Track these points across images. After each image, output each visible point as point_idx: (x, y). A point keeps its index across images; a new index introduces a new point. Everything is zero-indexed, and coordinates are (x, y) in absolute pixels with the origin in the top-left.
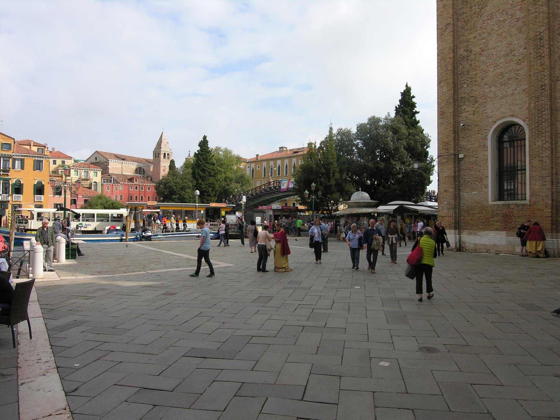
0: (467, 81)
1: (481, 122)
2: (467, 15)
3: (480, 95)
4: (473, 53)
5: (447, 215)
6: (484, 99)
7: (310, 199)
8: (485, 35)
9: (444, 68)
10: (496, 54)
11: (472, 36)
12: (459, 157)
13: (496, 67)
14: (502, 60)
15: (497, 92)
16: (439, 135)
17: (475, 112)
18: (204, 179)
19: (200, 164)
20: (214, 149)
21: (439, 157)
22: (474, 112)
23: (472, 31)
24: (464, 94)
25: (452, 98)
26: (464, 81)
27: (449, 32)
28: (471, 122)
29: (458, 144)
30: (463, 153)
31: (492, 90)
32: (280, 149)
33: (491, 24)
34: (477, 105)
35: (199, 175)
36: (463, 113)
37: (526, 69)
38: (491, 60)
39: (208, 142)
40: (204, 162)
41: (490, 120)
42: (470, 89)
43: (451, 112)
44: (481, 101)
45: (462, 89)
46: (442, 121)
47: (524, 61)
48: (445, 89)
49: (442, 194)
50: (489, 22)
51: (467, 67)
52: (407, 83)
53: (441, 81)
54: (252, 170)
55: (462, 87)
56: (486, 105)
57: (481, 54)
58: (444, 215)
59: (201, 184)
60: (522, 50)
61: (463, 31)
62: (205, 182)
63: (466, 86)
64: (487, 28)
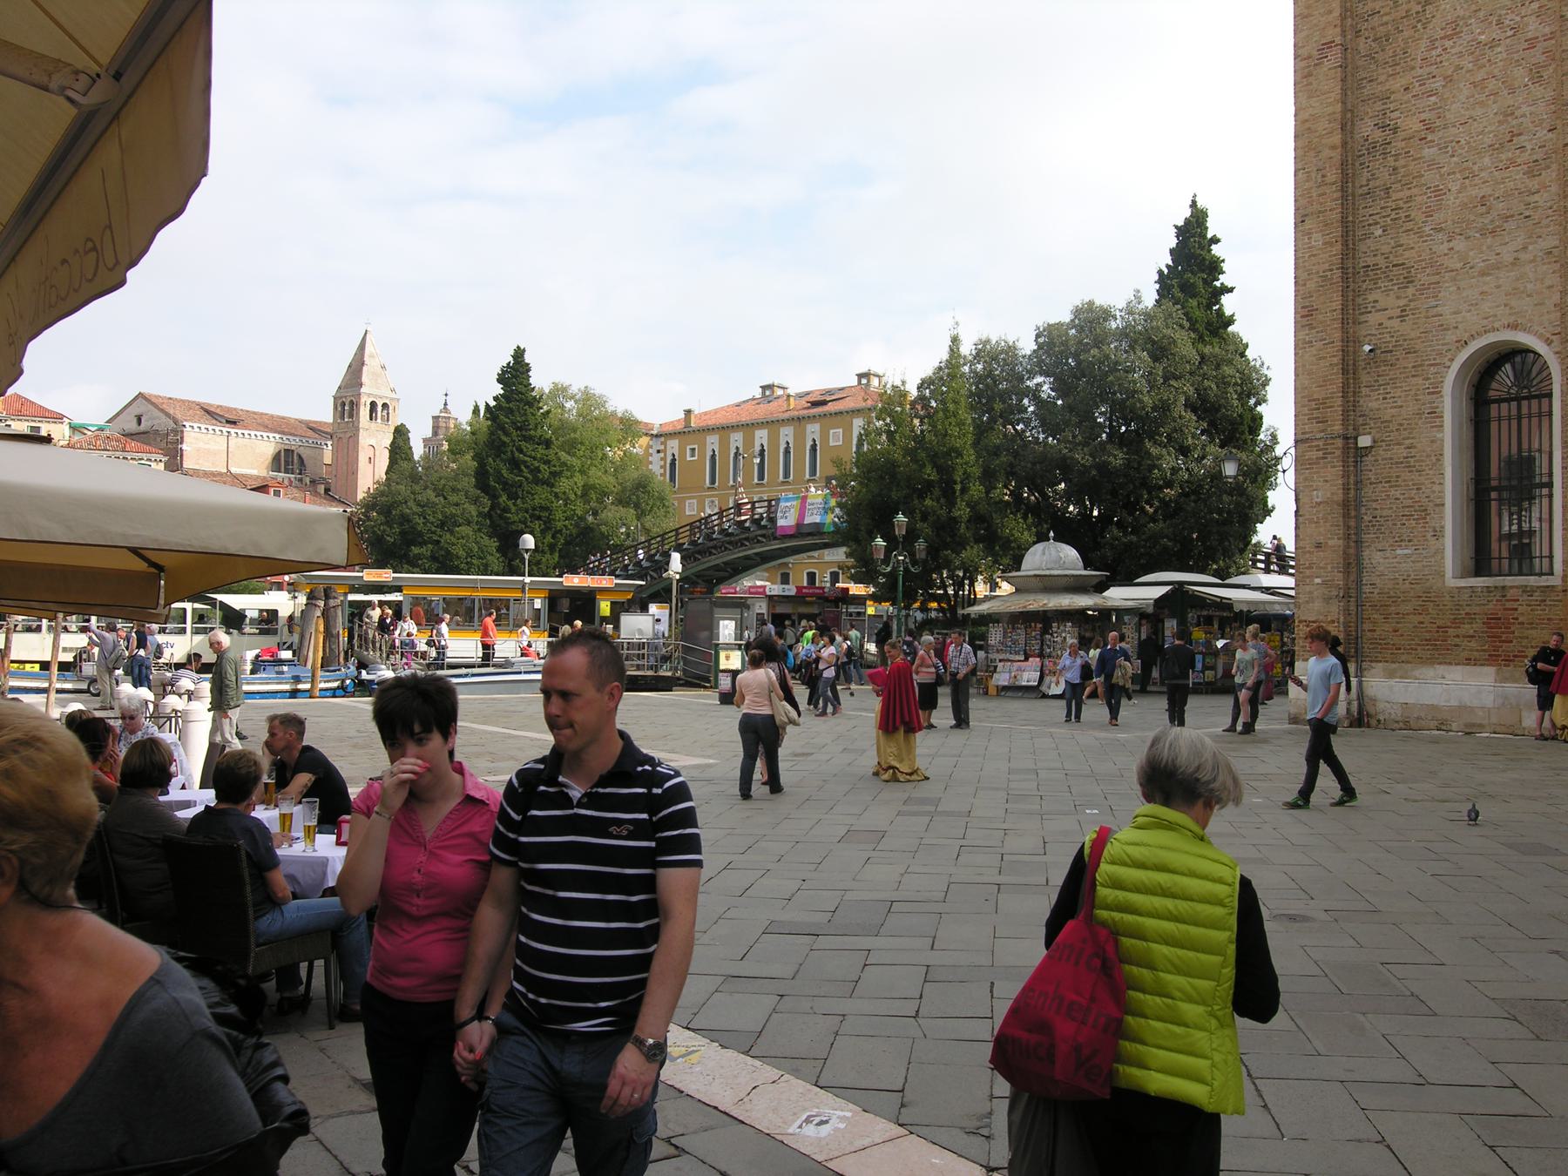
0: (1384, 217)
1: (1423, 342)
3: (1423, 260)
4: (1401, 135)
6: (1433, 275)
7: (891, 565)
9: (1313, 175)
11: (1397, 84)
12: (1360, 445)
13: (1467, 181)
14: (1487, 160)
15: (1471, 253)
16: (1301, 377)
17: (1405, 310)
18: (516, 493)
19: (504, 443)
21: (1300, 445)
22: (1402, 311)
23: (1398, 67)
24: (1375, 255)
25: (1337, 269)
26: (1374, 217)
27: (1330, 69)
28: (1394, 340)
29: (1354, 406)
30: (1370, 433)
31: (1457, 249)
32: (764, 393)
33: (1453, 51)
34: (1411, 291)
35: (499, 478)
36: (1370, 312)
37: (1554, 189)
38: (1455, 159)
39: (529, 370)
40: (518, 436)
41: (1451, 337)
42: (1392, 242)
43: (1335, 310)
44: (1423, 278)
46: (1307, 335)
47: (1548, 167)
48: (1317, 240)
49: (1308, 555)
50: (1448, 44)
51: (1384, 176)
52: (1195, 196)
53: (1306, 215)
54: (668, 461)
55: (1367, 236)
56: (1440, 292)
57: (1425, 138)
59: (506, 510)
60: (1542, 133)
61: (1373, 67)
62: (519, 501)
63: (1379, 232)
64: (1441, 62)
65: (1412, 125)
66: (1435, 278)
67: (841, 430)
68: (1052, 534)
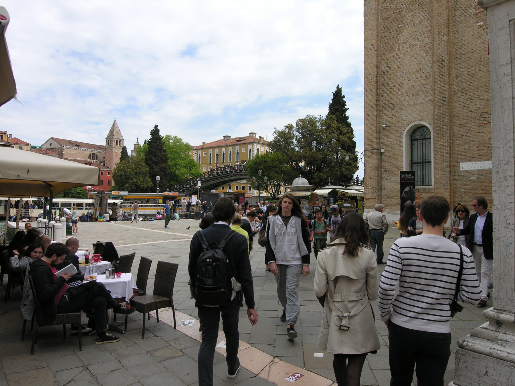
2: (388, 38)
4: (392, 69)
5: (371, 197)
8: (401, 56)
10: (409, 71)
11: (391, 55)
14: (414, 76)
15: (410, 101)
20: (165, 137)
21: (366, 151)
23: (391, 51)
32: (224, 138)
33: (406, 47)
34: (394, 110)
37: (431, 83)
38: (406, 75)
39: (159, 131)
41: (405, 123)
44: (398, 107)
45: (383, 97)
47: (430, 78)
48: (370, 97)
50: (404, 45)
51: (387, 80)
52: (338, 85)
54: (198, 156)
55: (383, 96)
60: (429, 69)
61: (385, 51)
63: (386, 95)
65: (394, 66)
66: (401, 107)
68: (300, 175)
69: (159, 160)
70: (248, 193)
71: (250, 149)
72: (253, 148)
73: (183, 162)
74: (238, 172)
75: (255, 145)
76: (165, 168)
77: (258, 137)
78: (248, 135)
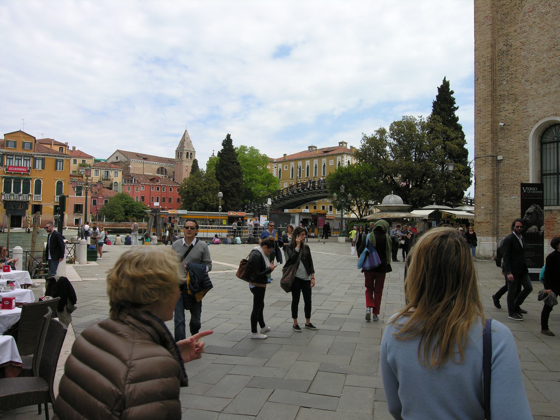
0: (507, 77)
1: (521, 121)
2: (507, 7)
3: (521, 92)
5: (484, 221)
6: (525, 97)
8: (527, 29)
9: (481, 63)
10: (538, 49)
11: (512, 29)
12: (498, 159)
13: (537, 63)
14: (545, 55)
15: (539, 89)
16: (477, 135)
17: (515, 110)
20: (239, 148)
21: (476, 159)
22: (514, 111)
23: (512, 24)
24: (503, 91)
25: (490, 96)
26: (503, 78)
27: (487, 26)
28: (510, 121)
29: (496, 145)
30: (502, 155)
31: (534, 87)
32: (309, 149)
33: (532, 16)
34: (517, 103)
36: (502, 111)
38: (533, 55)
39: (232, 141)
41: (532, 119)
42: (510, 86)
43: (489, 111)
44: (522, 99)
45: (501, 86)
46: (479, 120)
48: (483, 86)
50: (530, 14)
53: (479, 78)
54: (279, 171)
55: (500, 85)
56: (528, 103)
57: (522, 48)
58: (481, 221)
63: (505, 83)
64: (528, 21)
65: (517, 44)
66: (526, 98)
67: (333, 160)
68: (392, 192)
69: (231, 175)
70: (336, 213)
71: (339, 162)
72: (343, 161)
73: (259, 177)
74: (322, 188)
75: (345, 156)
76: (238, 184)
77: (349, 148)
78: (338, 145)
